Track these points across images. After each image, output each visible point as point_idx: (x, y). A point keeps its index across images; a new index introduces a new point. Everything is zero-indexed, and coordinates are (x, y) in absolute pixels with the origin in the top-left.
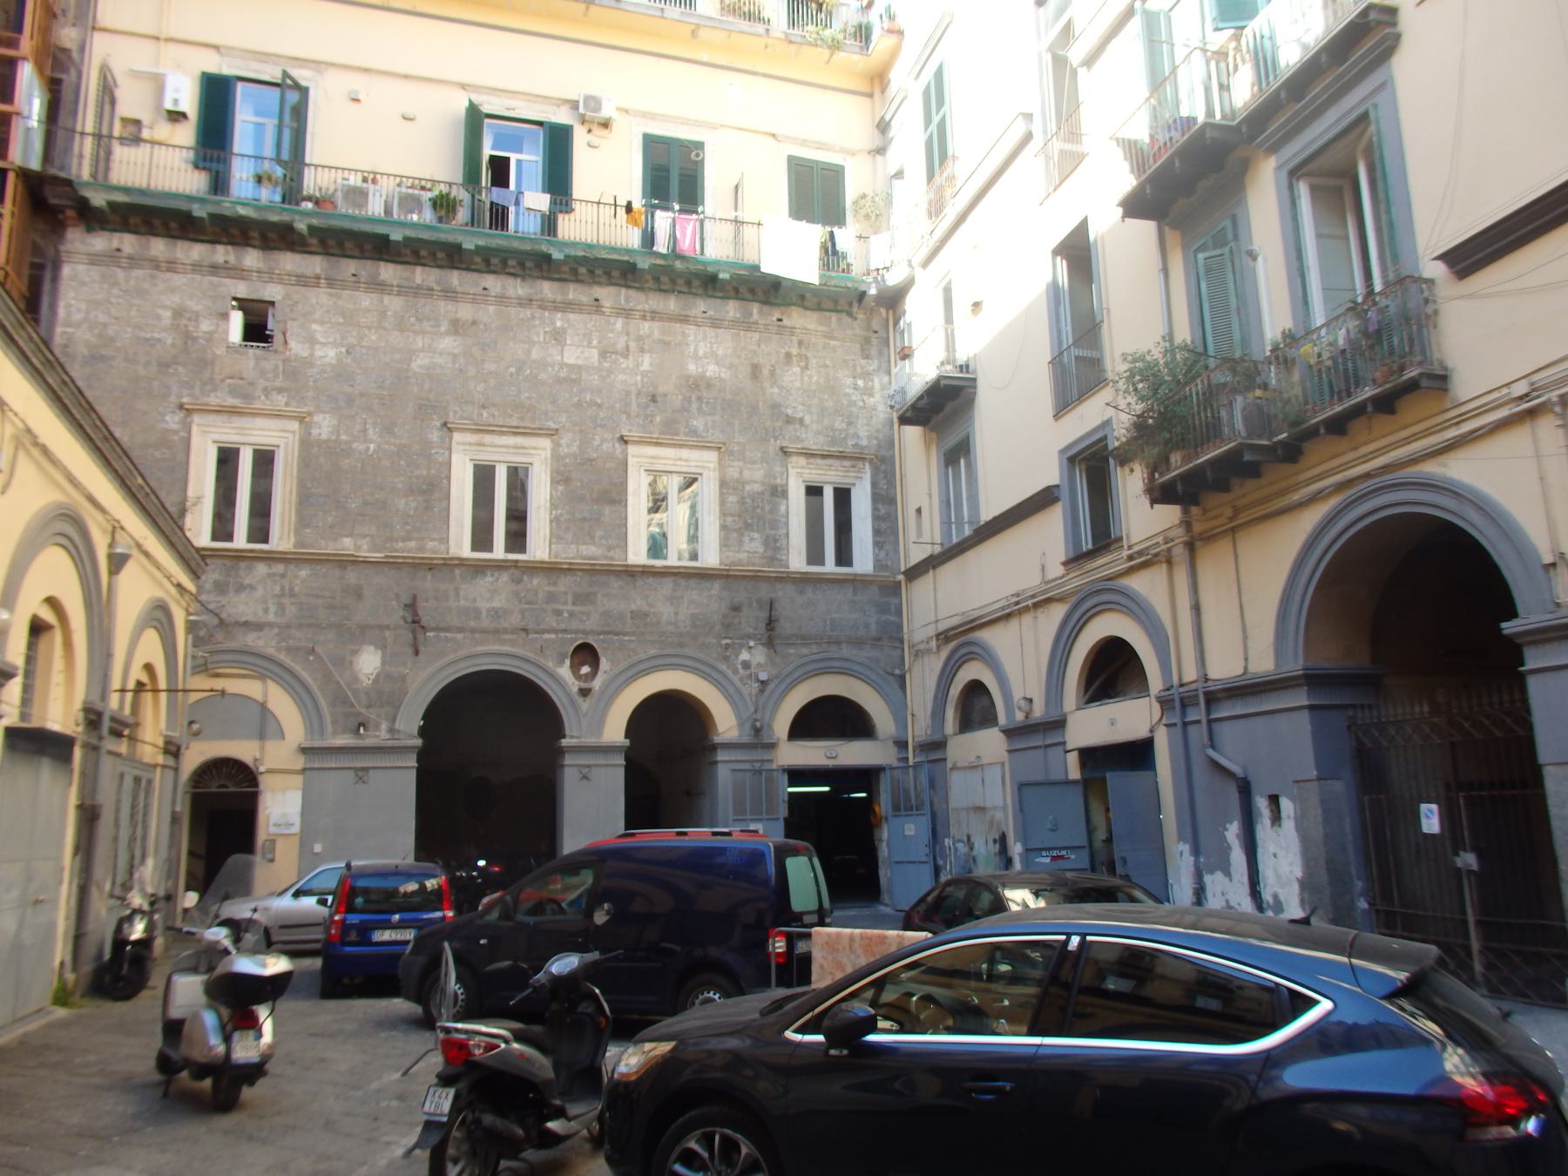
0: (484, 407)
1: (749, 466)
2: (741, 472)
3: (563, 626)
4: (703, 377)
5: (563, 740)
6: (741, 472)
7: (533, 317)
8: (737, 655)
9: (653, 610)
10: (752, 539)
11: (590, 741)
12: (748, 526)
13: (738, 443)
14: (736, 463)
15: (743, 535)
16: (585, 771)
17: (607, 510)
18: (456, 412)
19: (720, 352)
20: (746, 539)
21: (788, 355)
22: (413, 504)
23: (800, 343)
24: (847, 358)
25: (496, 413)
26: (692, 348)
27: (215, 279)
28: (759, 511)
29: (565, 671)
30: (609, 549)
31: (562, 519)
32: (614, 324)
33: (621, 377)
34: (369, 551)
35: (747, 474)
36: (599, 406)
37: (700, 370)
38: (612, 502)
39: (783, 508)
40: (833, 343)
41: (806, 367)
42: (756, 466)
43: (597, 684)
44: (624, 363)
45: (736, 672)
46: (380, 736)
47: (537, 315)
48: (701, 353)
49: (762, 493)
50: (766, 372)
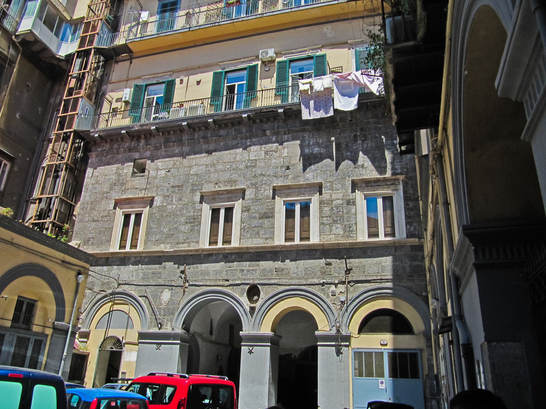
0: (216, 184)
1: (335, 192)
2: (331, 196)
3: (244, 277)
4: (312, 154)
5: (241, 332)
6: (331, 196)
7: (238, 143)
8: (329, 288)
9: (286, 267)
10: (337, 228)
11: (254, 332)
12: (335, 222)
13: (329, 182)
14: (328, 191)
15: (332, 226)
16: (251, 348)
17: (266, 221)
18: (205, 187)
19: (320, 142)
20: (334, 228)
21: (355, 137)
22: (187, 228)
23: (362, 129)
24: (388, 131)
25: (221, 186)
26: (307, 142)
27: (130, 154)
28: (341, 213)
29: (244, 300)
30: (266, 239)
31: (246, 227)
32: (272, 139)
33: (274, 161)
34: (170, 249)
35: (334, 196)
36: (264, 175)
37: (311, 151)
38: (268, 217)
39: (353, 211)
40: (379, 126)
41: (365, 140)
42: (339, 192)
43: (258, 305)
44: (276, 155)
45: (328, 296)
46: (167, 329)
47: (240, 142)
48: (311, 143)
49: (342, 204)
50: (343, 146)
